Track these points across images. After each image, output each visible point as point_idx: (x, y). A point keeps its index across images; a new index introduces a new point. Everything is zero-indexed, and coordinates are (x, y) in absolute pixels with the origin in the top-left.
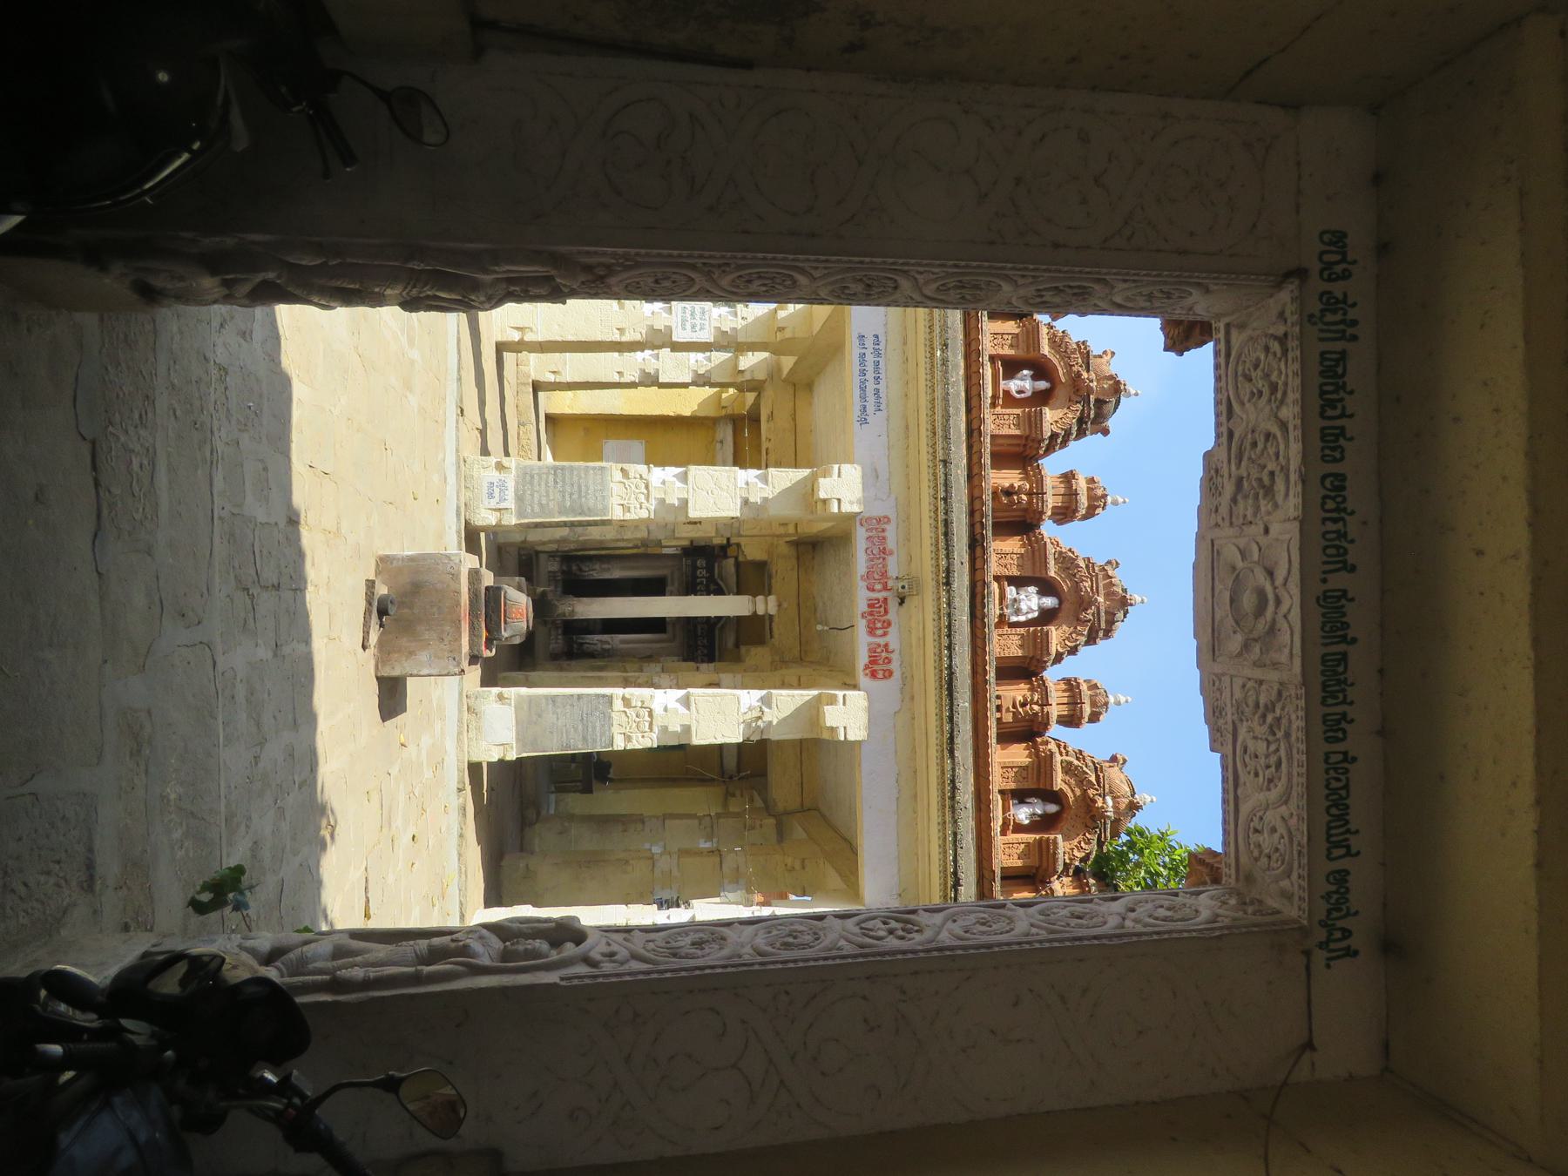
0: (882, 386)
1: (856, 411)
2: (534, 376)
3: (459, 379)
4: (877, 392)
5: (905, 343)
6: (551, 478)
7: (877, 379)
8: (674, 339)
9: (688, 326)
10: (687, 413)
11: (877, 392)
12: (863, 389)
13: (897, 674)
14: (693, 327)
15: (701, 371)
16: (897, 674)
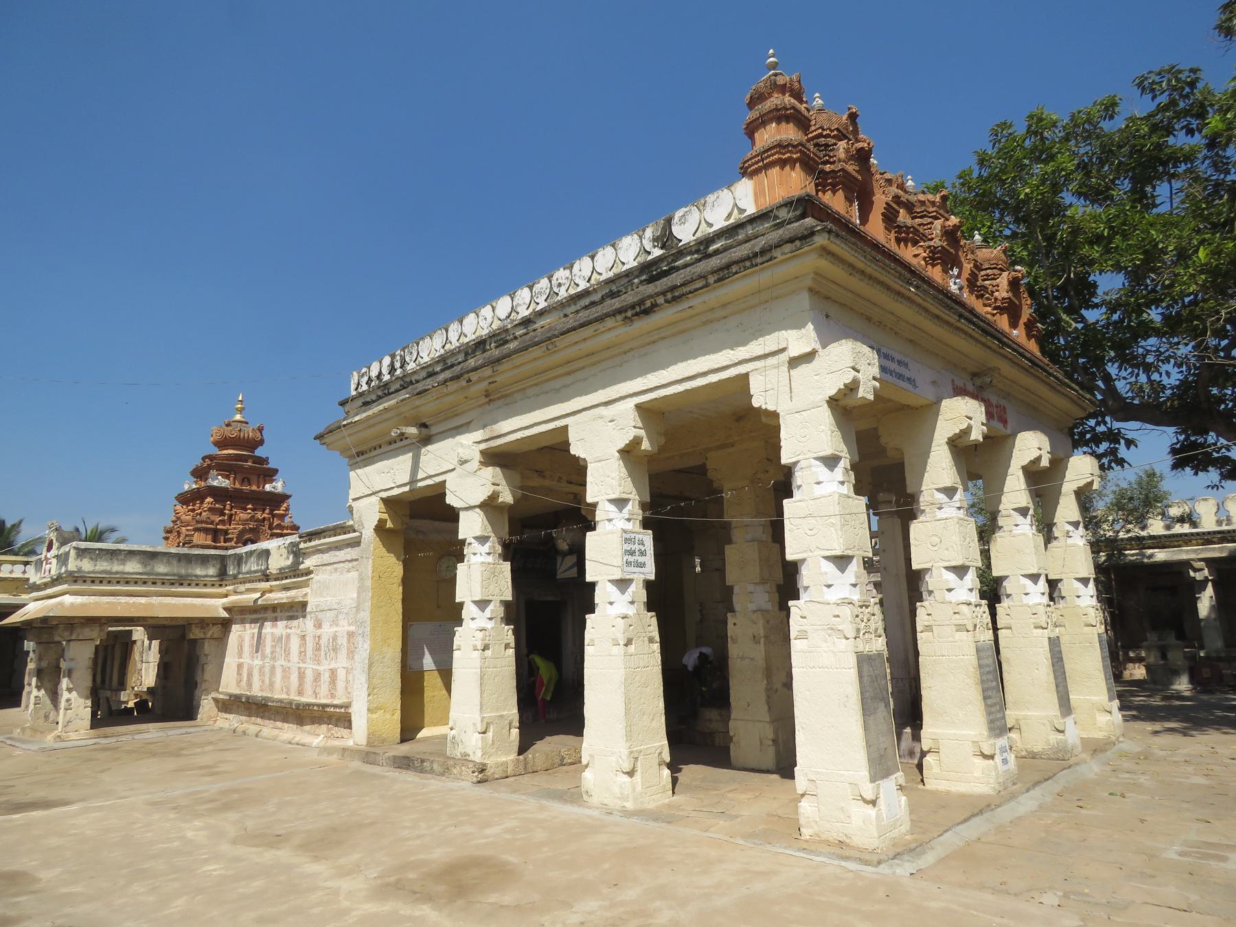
0: (897, 356)
1: (910, 387)
2: (513, 756)
3: (981, 812)
4: (899, 362)
5: (869, 319)
6: (989, 702)
7: (893, 359)
8: (652, 577)
9: (641, 559)
10: (398, 570)
11: (899, 362)
12: (900, 376)
13: (1003, 402)
14: (643, 553)
15: (499, 549)
16: (1003, 402)
